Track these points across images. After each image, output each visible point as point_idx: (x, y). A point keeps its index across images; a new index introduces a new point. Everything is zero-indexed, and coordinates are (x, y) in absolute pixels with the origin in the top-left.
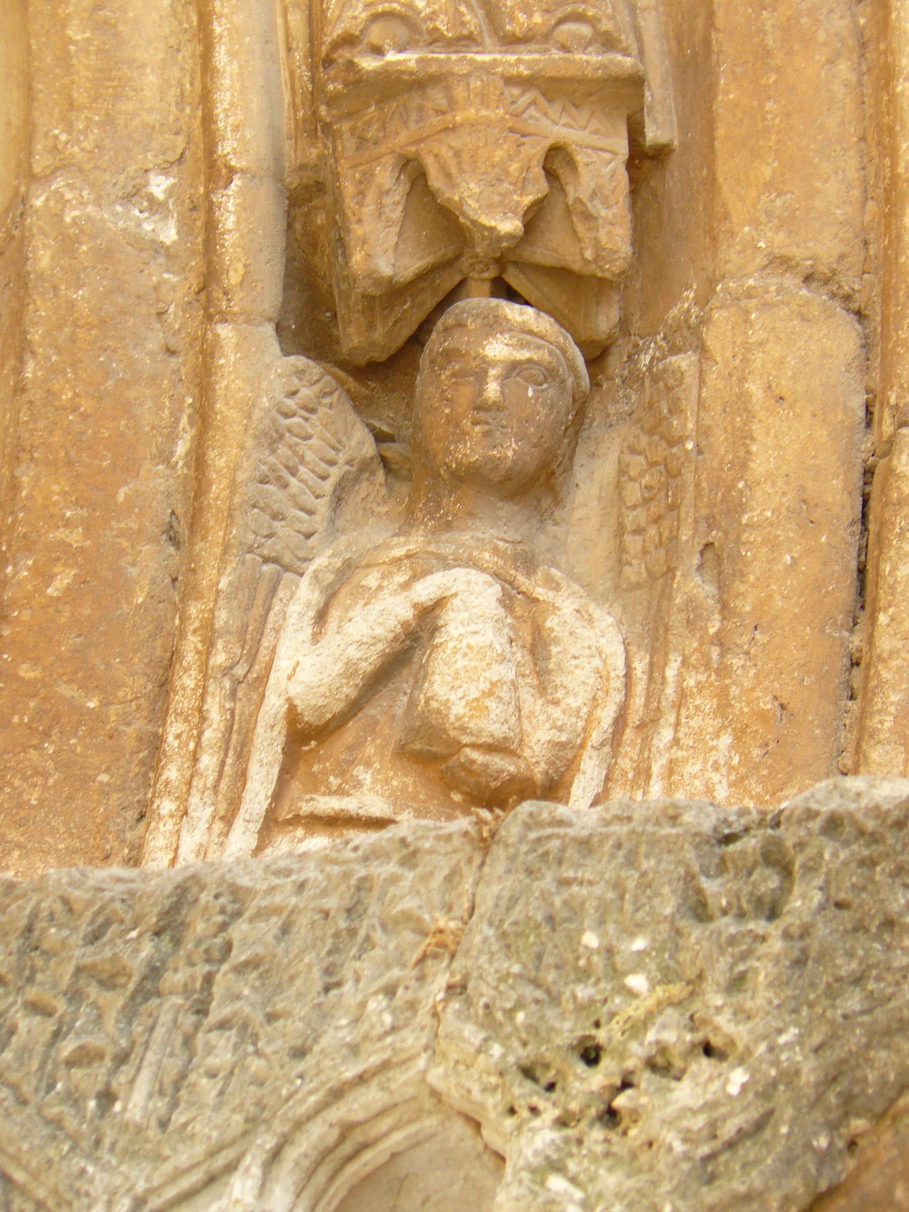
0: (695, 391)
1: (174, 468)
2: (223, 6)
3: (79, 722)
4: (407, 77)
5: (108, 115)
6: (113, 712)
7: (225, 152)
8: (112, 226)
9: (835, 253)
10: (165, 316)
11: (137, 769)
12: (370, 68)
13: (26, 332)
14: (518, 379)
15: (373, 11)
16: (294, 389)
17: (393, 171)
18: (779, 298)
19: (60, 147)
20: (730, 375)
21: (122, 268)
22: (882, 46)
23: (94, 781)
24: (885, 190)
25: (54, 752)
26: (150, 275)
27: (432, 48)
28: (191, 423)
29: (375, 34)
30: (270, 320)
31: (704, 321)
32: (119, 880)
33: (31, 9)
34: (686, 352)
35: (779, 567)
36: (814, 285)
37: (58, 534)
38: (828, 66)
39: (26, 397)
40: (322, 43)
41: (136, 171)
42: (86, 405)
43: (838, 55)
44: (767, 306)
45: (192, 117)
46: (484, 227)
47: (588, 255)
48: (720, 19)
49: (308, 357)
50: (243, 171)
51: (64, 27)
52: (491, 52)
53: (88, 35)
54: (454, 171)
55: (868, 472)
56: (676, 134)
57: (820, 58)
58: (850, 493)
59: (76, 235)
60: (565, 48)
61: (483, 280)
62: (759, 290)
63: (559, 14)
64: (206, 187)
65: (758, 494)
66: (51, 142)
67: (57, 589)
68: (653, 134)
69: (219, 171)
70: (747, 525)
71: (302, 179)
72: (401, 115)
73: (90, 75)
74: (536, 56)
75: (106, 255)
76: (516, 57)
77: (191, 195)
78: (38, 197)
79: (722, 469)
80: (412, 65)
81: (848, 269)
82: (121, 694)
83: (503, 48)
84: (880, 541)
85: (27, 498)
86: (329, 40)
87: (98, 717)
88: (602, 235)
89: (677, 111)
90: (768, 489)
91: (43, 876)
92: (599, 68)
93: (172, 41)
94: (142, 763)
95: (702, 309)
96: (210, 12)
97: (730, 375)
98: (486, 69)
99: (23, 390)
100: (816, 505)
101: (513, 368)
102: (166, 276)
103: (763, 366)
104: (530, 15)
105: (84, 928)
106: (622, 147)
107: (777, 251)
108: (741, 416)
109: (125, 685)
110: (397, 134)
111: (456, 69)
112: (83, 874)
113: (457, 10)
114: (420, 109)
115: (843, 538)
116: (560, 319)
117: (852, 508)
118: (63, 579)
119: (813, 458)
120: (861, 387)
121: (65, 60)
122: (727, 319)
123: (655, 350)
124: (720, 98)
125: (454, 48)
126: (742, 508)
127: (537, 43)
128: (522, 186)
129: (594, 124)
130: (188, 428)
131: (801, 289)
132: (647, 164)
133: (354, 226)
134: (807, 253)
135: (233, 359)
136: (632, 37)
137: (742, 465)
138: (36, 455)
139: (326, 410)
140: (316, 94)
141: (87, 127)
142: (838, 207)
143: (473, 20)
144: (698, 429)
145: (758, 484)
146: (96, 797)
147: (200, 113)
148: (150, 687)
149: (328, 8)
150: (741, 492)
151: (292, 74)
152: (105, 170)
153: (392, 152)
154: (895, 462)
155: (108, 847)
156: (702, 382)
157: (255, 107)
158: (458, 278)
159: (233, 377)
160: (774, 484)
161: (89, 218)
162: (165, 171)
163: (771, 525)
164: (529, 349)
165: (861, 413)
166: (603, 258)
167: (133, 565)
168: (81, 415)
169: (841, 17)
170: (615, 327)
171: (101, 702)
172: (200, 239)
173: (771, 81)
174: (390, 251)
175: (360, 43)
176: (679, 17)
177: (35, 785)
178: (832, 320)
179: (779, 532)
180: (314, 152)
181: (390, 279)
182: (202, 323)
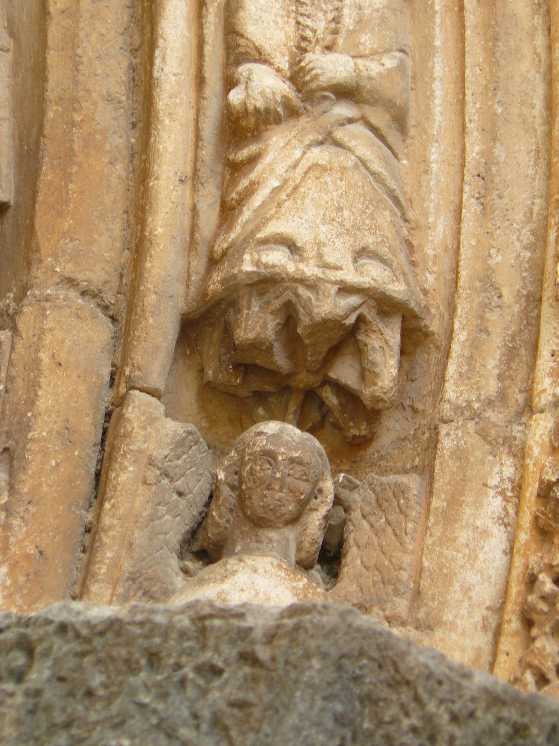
0: (7, 354)
9: (102, 279)
20: (30, 346)
22: (143, 157)
24: (136, 244)
31: (18, 312)
34: (5, 329)
35: (48, 467)
36: (87, 298)
38: (110, 166)
43: (116, 159)
48: (47, 130)
55: (108, 415)
56: (13, 197)
58: (95, 427)
62: (53, 297)
65: (39, 421)
70: (31, 440)
79: (19, 404)
81: (108, 290)
84: (111, 458)
89: (15, 183)
90: (46, 419)
95: (17, 305)
97: (30, 346)
100: (74, 432)
103: (50, 343)
107: (66, 274)
108: (34, 373)
115: (88, 454)
117: (96, 436)
119: (75, 402)
120: (109, 363)
122: (31, 313)
124: (42, 178)
126: (29, 428)
131: (78, 299)
137: (31, 402)
144: (7, 377)
150: (29, 419)
154: (125, 411)
156: (13, 349)
163: (45, 441)
165: (107, 378)
169: (120, 137)
173: (73, 171)
176: (22, 126)
178: (95, 320)
179: (50, 446)
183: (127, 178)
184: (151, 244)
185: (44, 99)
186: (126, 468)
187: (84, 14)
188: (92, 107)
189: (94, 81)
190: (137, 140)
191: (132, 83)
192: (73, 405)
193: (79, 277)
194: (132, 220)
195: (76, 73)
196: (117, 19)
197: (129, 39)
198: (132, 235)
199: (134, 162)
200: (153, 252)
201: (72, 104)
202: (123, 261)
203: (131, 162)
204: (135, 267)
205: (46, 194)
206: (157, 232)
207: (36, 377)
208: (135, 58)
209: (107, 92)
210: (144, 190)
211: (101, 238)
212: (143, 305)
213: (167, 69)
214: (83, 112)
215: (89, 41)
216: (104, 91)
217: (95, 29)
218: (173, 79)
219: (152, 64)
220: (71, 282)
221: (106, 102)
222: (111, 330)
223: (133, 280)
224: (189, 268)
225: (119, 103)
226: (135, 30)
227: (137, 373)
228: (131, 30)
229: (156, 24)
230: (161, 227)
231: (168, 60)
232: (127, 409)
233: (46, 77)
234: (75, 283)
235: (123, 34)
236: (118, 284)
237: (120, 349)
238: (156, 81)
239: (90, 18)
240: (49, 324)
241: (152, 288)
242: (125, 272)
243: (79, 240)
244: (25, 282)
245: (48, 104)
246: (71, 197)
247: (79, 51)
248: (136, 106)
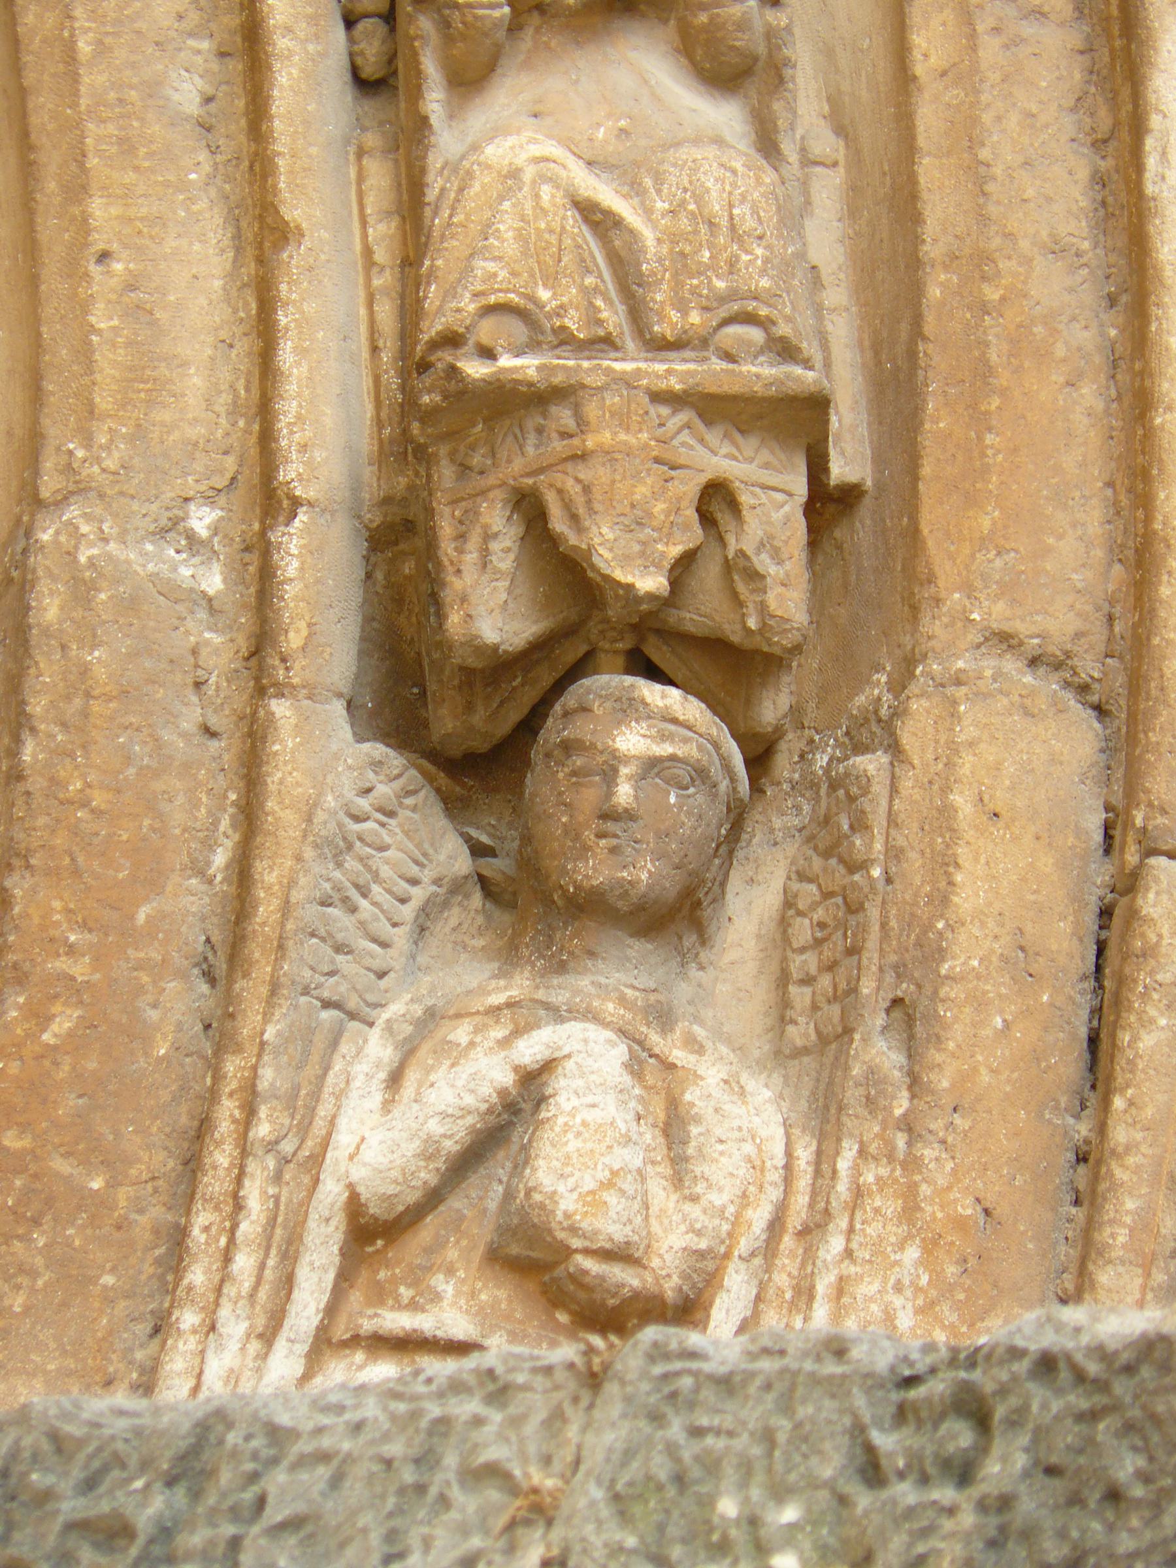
0: (884, 803)
1: (210, 882)
2: (290, 291)
3: (79, 1208)
4: (524, 389)
5: (139, 426)
6: (123, 1195)
7: (288, 478)
8: (139, 569)
9: (1070, 629)
10: (204, 687)
11: (151, 1270)
12: (477, 376)
13: (24, 702)
14: (658, 780)
15: (484, 302)
16: (368, 785)
17: (504, 507)
19: (75, 465)
21: (152, 624)
23: (96, 1284)
24: (1137, 551)
25: (46, 1245)
26: (188, 633)
27: (558, 352)
28: (234, 826)
29: (486, 332)
30: (340, 695)
31: (898, 713)
32: (121, 1413)
33: (43, 287)
34: (874, 751)
35: (987, 1032)
36: (1042, 670)
37: (58, 964)
39: (21, 787)
40: (416, 343)
41: (172, 499)
42: (99, 799)
43: (1081, 375)
45: (247, 431)
46: (619, 583)
47: (752, 623)
49: (388, 745)
50: (310, 504)
51: (86, 312)
52: (633, 359)
53: (115, 322)
54: (581, 511)
55: (1106, 913)
56: (869, 470)
58: (1081, 940)
59: (92, 579)
60: (729, 357)
61: (616, 652)
63: (723, 313)
64: (262, 522)
65: (962, 937)
66: (64, 460)
67: (55, 1035)
68: (840, 470)
69: (280, 502)
70: (947, 977)
71: (385, 516)
72: (516, 437)
73: (117, 374)
74: (692, 366)
75: (131, 605)
76: (665, 367)
77: (243, 532)
78: (44, 530)
79: (916, 904)
80: (532, 373)
81: (1086, 651)
82: (133, 1172)
83: (650, 355)
84: (1118, 1002)
85: (20, 916)
86: (426, 337)
87: (103, 1201)
88: (771, 599)
89: (871, 442)
91: (24, 1406)
92: (771, 384)
93: (223, 334)
94: (158, 1262)
95: (896, 698)
96: (274, 297)
97: (930, 782)
98: (627, 382)
99: (20, 778)
100: (1037, 954)
101: (652, 766)
102: (207, 635)
104: (685, 313)
105: (77, 1473)
106: (800, 486)
107: (994, 626)
108: (943, 837)
109: (139, 1160)
110: (509, 461)
111: (588, 381)
112: (77, 1406)
113: (591, 304)
114: (540, 431)
115: (1071, 998)
116: (714, 705)
117: (1083, 959)
118: (63, 1022)
119: (1035, 892)
120: (1099, 804)
121: (85, 354)
123: (834, 747)
124: (927, 426)
125: (587, 353)
126: (941, 954)
127: (693, 349)
128: (667, 532)
129: (765, 455)
130: (230, 832)
131: (1024, 674)
132: (832, 508)
133: (451, 578)
134: (1034, 629)
135: (290, 744)
136: (815, 343)
137: (942, 900)
138: (33, 861)
139: (409, 813)
140: (409, 406)
141: (111, 441)
142: (1075, 571)
143: (613, 317)
144: (887, 851)
145: (963, 924)
146: (97, 1305)
147: (256, 427)
148: (171, 1163)
149: (426, 298)
151: (377, 380)
152: (133, 497)
153: (504, 484)
154: (1140, 902)
155: (111, 1369)
156: (894, 790)
157: (328, 422)
158: (583, 649)
159: (289, 768)
161: (110, 557)
162: (209, 500)
163: (978, 977)
164: (672, 741)
165: (1098, 837)
166: (771, 627)
167: (154, 1006)
168: (92, 811)
170: (785, 716)
171: (107, 1182)
172: (252, 590)
173: (993, 407)
174: (497, 611)
175: (465, 344)
177: (18, 1287)
179: (988, 987)
180: (403, 481)
181: (495, 648)
182: (252, 697)
183: (1107, 411)
184: (1168, 546)
185: (918, 260)
186: (1152, 1021)
187: (989, 74)
190: (1122, 331)
191: (1102, 212)
193: (1021, 628)
194: (1124, 500)
195: (981, 201)
196: (1058, 79)
197: (1088, 120)
199: (1119, 377)
201: (979, 266)
202: (1111, 587)
204: (1139, 599)
207: (948, 846)
208: (1103, 158)
209: (1050, 235)
210: (1145, 435)
211: (1061, 543)
212: (1162, 677)
215: (1003, 131)
216: (1044, 234)
217: (1014, 105)
219: (1140, 168)
220: (1005, 640)
221: (1050, 256)
222: (1097, 735)
223: (1135, 626)
225: (1077, 255)
226: (1100, 99)
227: (1160, 820)
229: (1142, 83)
232: (1145, 897)
234: (1014, 642)
236: (1104, 638)
237: (1120, 774)
238: (1152, 204)
240: (966, 732)
242: (1117, 610)
244: (909, 647)
246: (991, 461)
247: (984, 154)
248: (1113, 258)
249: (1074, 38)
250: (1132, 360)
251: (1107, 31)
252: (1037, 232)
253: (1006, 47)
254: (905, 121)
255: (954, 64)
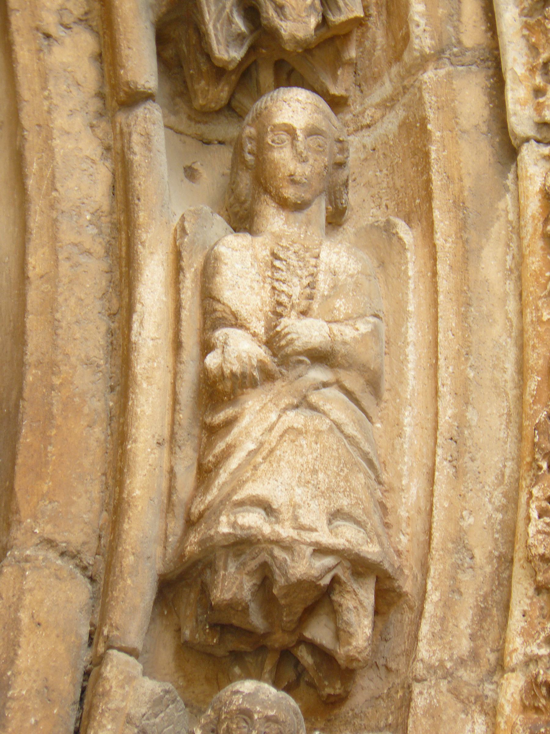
18: (44, 564)
20: (10, 607)
22: (121, 420)
24: (114, 506)
35: (27, 725)
36: (66, 558)
38: (88, 428)
43: (95, 422)
44: (37, 568)
55: (87, 674)
57: (84, 423)
58: (74, 685)
65: (19, 680)
70: (10, 698)
81: (87, 551)
84: (89, 716)
90: (26, 677)
97: (10, 607)
100: (53, 691)
103: (30, 604)
107: (45, 536)
115: (68, 713)
117: (75, 694)
119: (55, 661)
120: (88, 622)
122: (11, 574)
124: (21, 440)
126: (8, 687)
131: (58, 560)
134: (64, 539)
142: (85, 514)
145: (20, 674)
150: (9, 678)
154: (103, 670)
160: (29, 675)
163: (25, 699)
165: (86, 638)
169: (99, 400)
179: (29, 704)
183: (105, 440)
184: (129, 505)
185: (23, 363)
186: (104, 726)
187: (63, 279)
188: (71, 371)
189: (72, 346)
190: (116, 403)
191: (110, 348)
192: (52, 664)
193: (58, 538)
194: (110, 482)
195: (55, 337)
196: (95, 284)
197: (107, 304)
198: (110, 497)
199: (112, 425)
200: (131, 514)
202: (101, 522)
203: (110, 424)
204: (113, 529)
205: (25, 457)
206: (135, 494)
207: (15, 637)
208: (113, 322)
209: (86, 356)
212: (121, 566)
213: (144, 334)
214: (62, 376)
215: (68, 306)
216: (83, 355)
217: (73, 294)
218: (151, 343)
219: (130, 329)
220: (50, 543)
221: (85, 366)
222: (89, 591)
223: (111, 541)
224: (166, 530)
226: (113, 295)
227: (116, 633)
228: (109, 295)
230: (139, 490)
231: (146, 324)
232: (105, 668)
233: (26, 341)
234: (55, 544)
235: (101, 299)
236: (96, 545)
237: (99, 609)
238: (134, 346)
239: (69, 283)
240: (28, 584)
241: (130, 550)
242: (103, 533)
243: (58, 502)
244: (5, 543)
245: (27, 367)
246: (50, 459)
247: (58, 316)
248: (114, 369)
249: (104, 265)
250: (119, 417)
251: (119, 264)
252: (80, 354)
253: (72, 267)
254: (22, 297)
255: (47, 273)
